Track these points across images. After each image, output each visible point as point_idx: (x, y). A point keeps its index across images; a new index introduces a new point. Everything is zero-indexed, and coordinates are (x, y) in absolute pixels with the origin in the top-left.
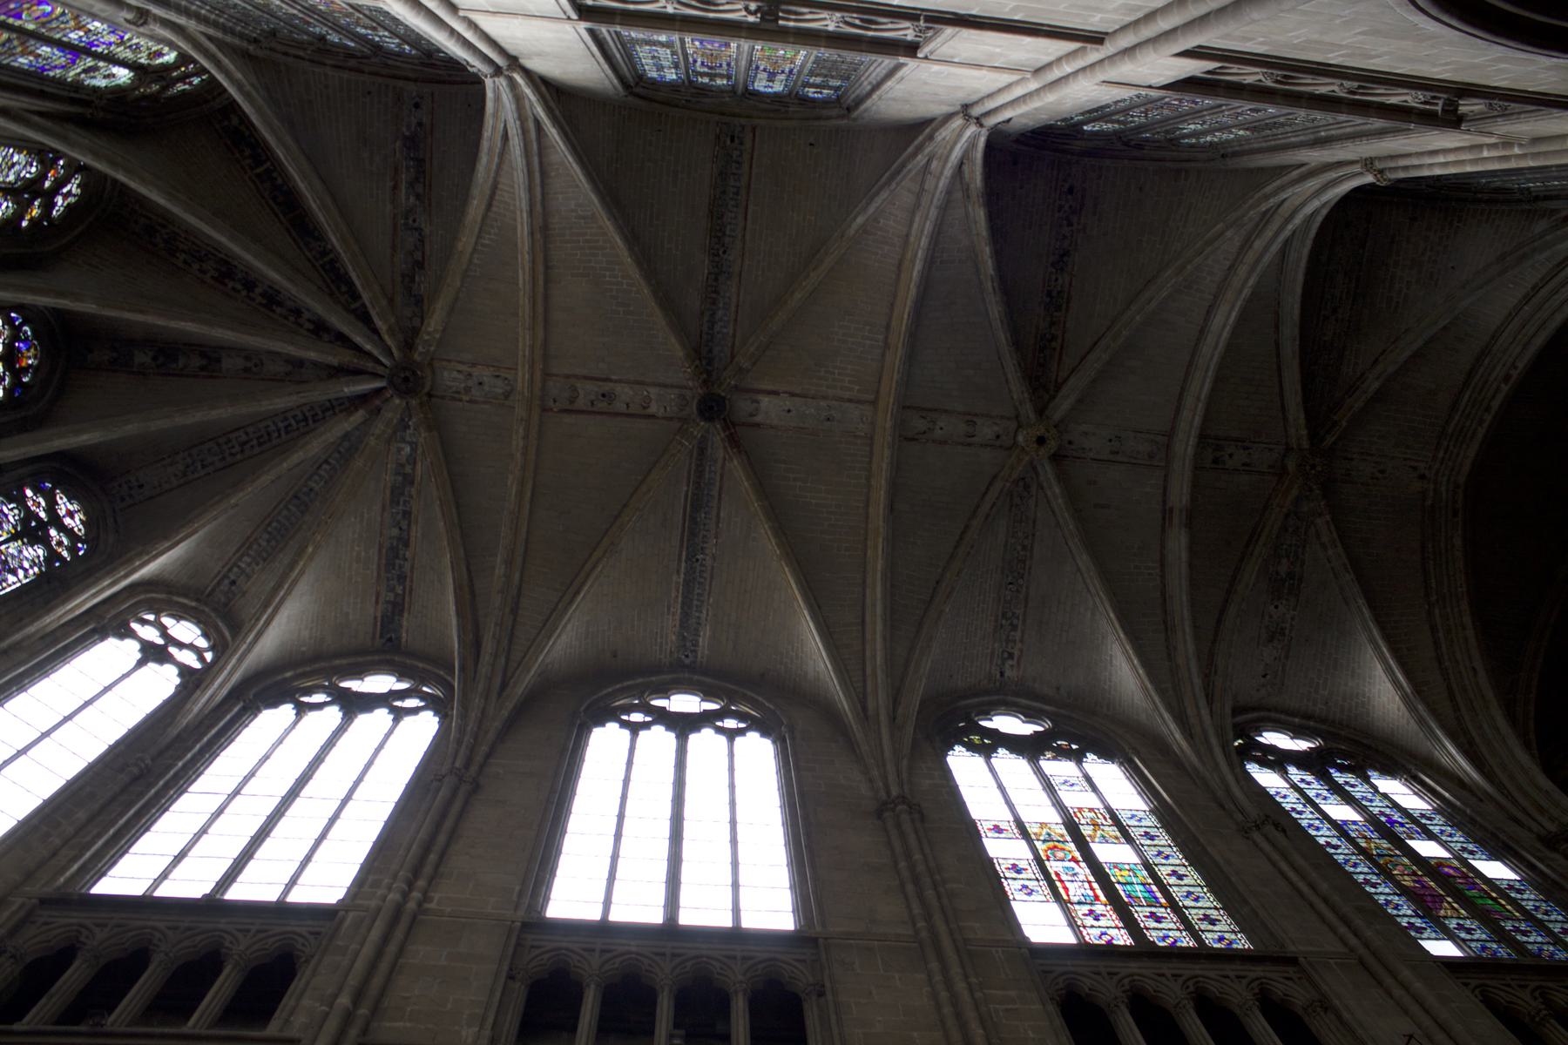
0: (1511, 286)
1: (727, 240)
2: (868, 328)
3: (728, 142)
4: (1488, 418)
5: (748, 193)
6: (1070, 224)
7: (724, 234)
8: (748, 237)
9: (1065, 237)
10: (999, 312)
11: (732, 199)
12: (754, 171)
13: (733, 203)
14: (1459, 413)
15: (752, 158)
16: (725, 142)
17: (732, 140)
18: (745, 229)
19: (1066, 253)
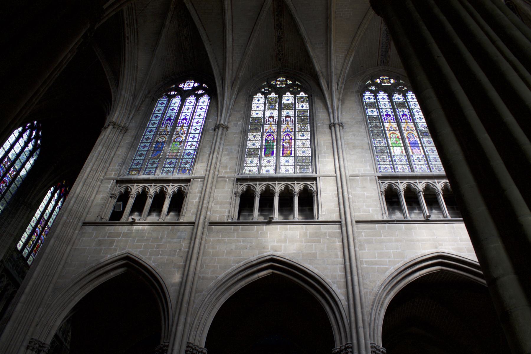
0: (143, 68)
1: (385, 33)
2: (342, 15)
3: (385, 61)
4: (126, 22)
5: (379, 47)
6: (279, 50)
7: (386, 34)
8: (379, 35)
9: (279, 46)
10: (301, 30)
11: (384, 45)
12: (377, 54)
13: (384, 44)
14: (134, 19)
15: (378, 57)
16: (386, 61)
17: (384, 61)
18: (380, 37)
19: (278, 42)
